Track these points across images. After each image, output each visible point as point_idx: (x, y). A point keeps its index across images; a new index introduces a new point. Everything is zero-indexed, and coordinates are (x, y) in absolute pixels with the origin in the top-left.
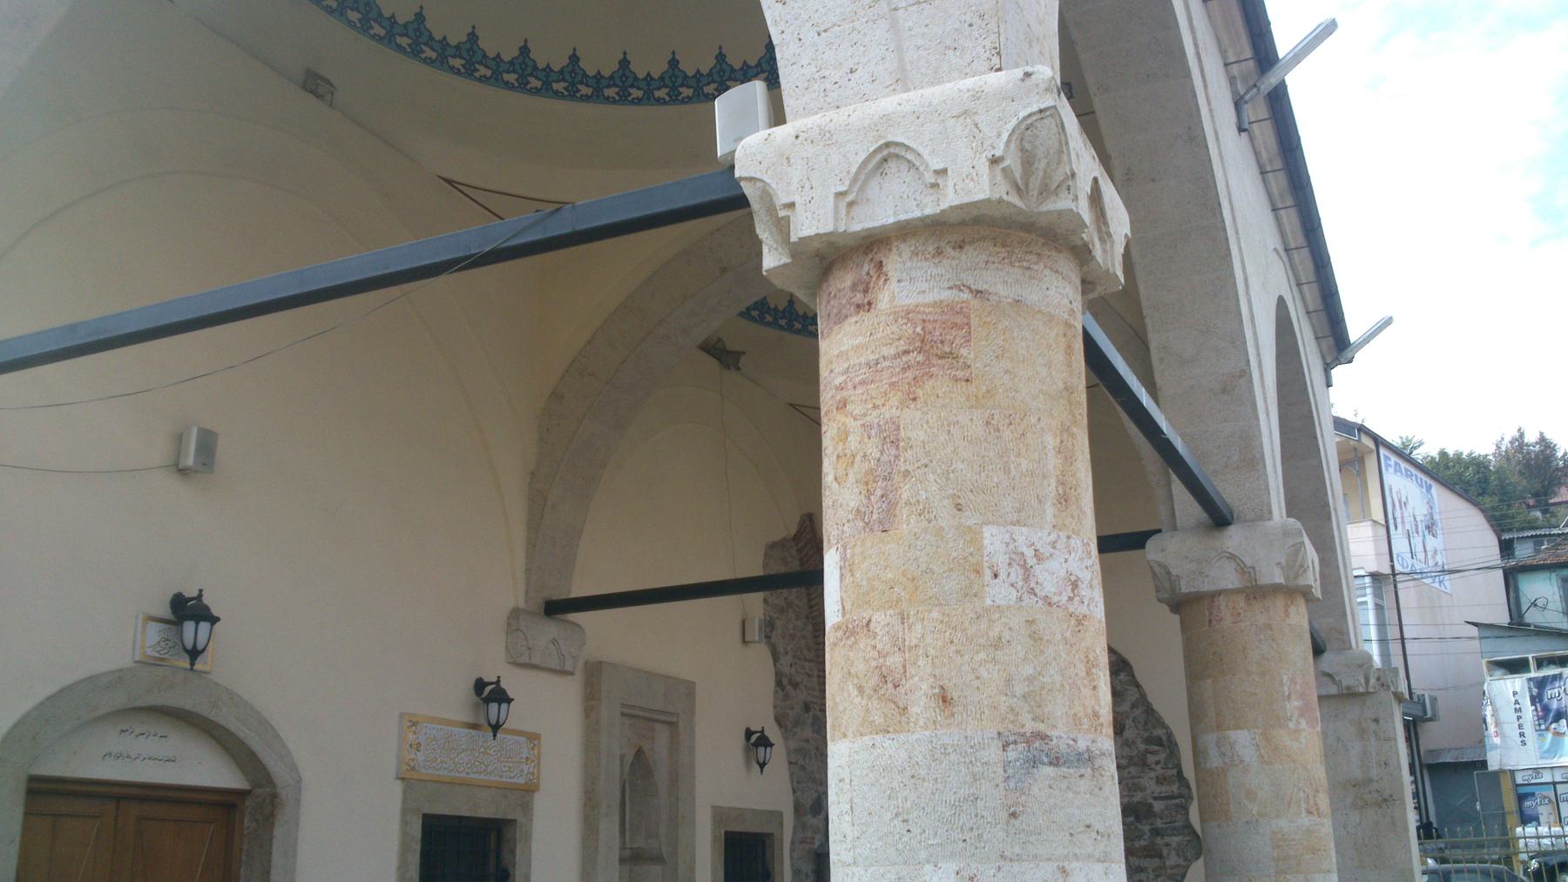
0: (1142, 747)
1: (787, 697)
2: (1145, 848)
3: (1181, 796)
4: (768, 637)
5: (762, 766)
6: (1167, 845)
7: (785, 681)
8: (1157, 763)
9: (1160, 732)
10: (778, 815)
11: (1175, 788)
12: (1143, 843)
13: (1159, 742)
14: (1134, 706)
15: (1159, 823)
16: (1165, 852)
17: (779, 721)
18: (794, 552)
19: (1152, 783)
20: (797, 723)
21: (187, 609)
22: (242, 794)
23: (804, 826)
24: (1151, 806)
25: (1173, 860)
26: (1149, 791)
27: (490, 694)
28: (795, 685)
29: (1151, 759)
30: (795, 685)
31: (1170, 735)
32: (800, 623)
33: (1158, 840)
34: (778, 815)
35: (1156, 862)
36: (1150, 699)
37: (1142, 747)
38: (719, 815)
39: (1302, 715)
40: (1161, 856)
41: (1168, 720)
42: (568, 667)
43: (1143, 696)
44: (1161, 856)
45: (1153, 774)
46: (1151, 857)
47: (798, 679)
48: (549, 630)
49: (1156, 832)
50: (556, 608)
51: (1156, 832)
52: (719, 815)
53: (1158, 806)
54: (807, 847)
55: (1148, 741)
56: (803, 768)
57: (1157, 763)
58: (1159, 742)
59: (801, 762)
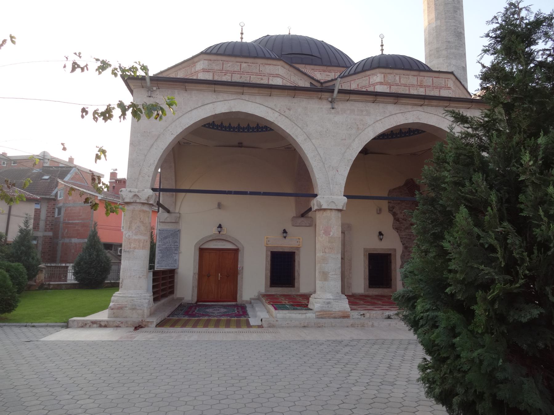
4: (390, 210)
5: (381, 239)
10: (395, 250)
17: (397, 229)
20: (407, 228)
21: (220, 226)
22: (238, 249)
27: (285, 231)
34: (395, 250)
38: (365, 250)
39: (324, 233)
42: (308, 225)
48: (302, 219)
50: (303, 215)
52: (365, 250)
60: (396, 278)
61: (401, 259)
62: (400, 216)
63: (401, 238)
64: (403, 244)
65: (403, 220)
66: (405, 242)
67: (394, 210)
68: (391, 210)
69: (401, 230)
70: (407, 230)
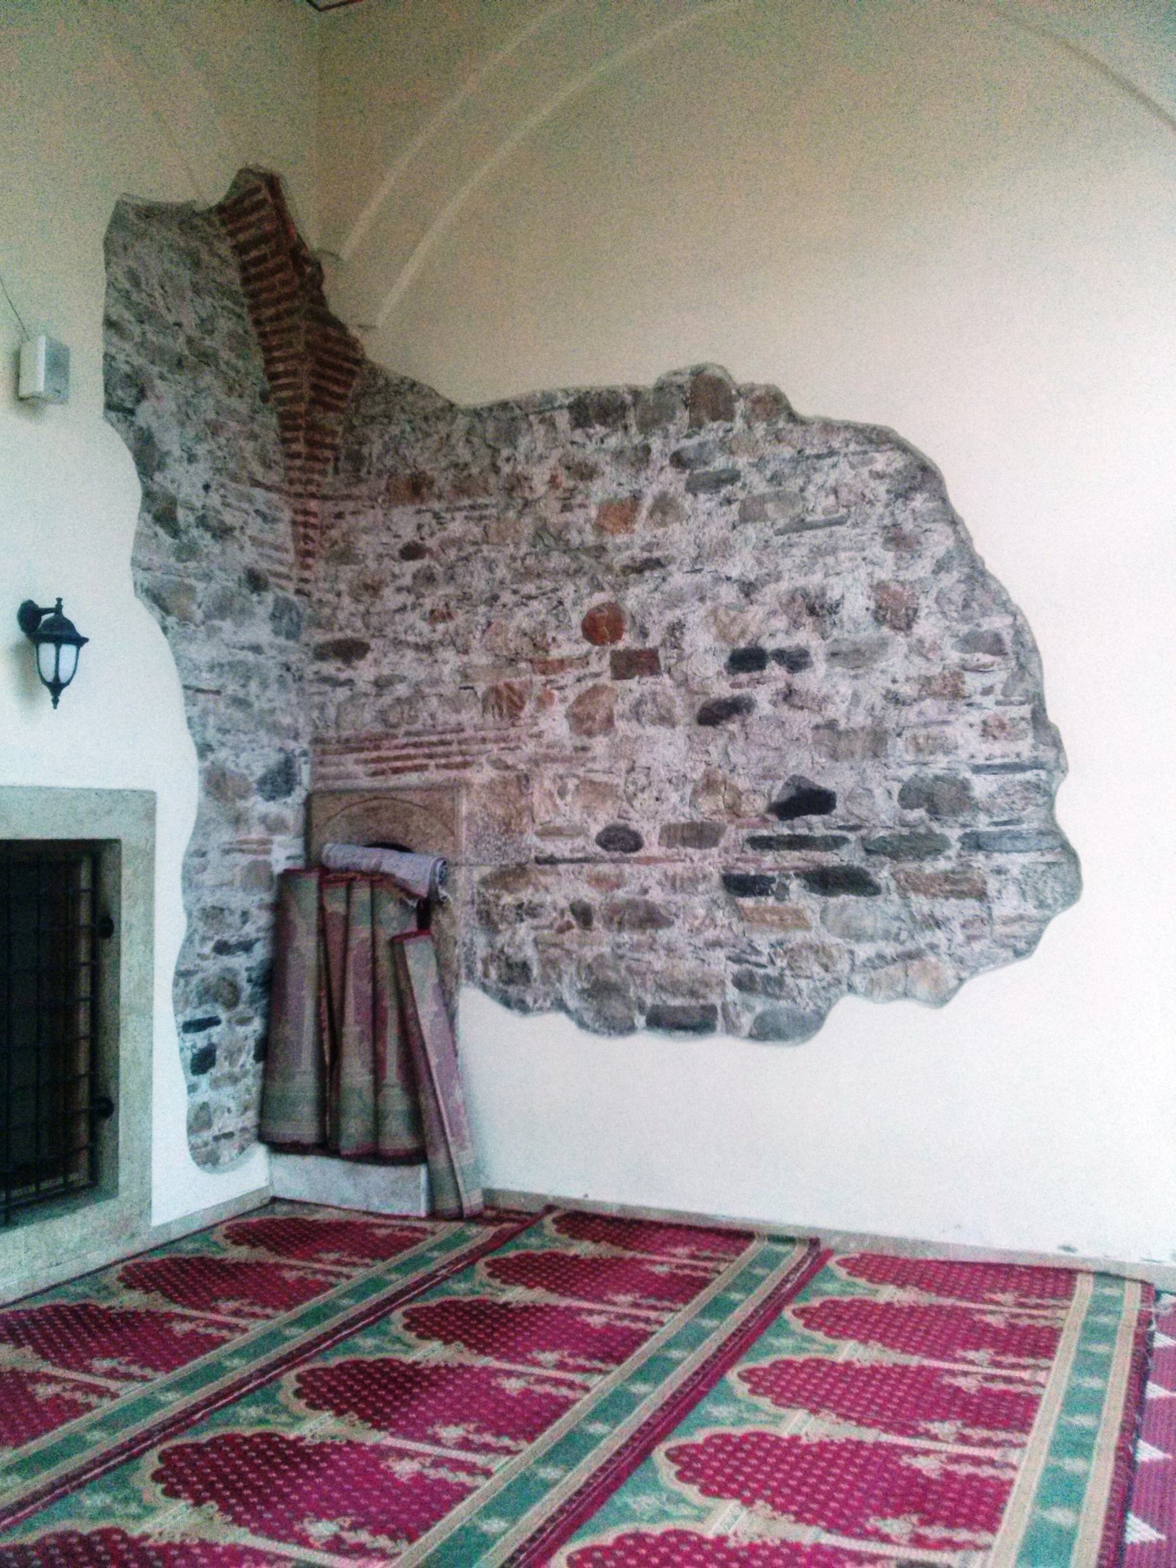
0: (954, 656)
1: (188, 552)
2: (947, 877)
3: (1037, 765)
5: (56, 687)
6: (999, 871)
7: (181, 514)
8: (987, 691)
9: (998, 623)
10: (146, 806)
11: (1024, 747)
12: (942, 865)
13: (996, 646)
14: (941, 567)
15: (983, 824)
16: (993, 885)
18: (224, 249)
19: (973, 735)
20: (223, 608)
23: (238, 820)
24: (965, 786)
25: (1008, 904)
26: (963, 755)
28: (222, 532)
29: (973, 683)
30: (222, 532)
31: (1020, 631)
32: (234, 402)
33: (978, 859)
34: (146, 806)
35: (971, 907)
36: (981, 547)
37: (954, 656)
40: (981, 895)
41: (1018, 595)
43: (964, 544)
44: (981, 895)
45: (975, 716)
46: (961, 895)
47: (229, 518)
49: (975, 843)
51: (975, 843)
53: (982, 786)
54: (244, 860)
55: (970, 642)
56: (241, 703)
57: (987, 691)
58: (996, 646)
59: (232, 688)
60: (146, 1085)
61: (189, 881)
62: (185, 482)
63: (192, 691)
64: (204, 749)
65: (202, 522)
66: (211, 735)
67: (145, 415)
68: (124, 397)
69: (185, 619)
70: (227, 625)
